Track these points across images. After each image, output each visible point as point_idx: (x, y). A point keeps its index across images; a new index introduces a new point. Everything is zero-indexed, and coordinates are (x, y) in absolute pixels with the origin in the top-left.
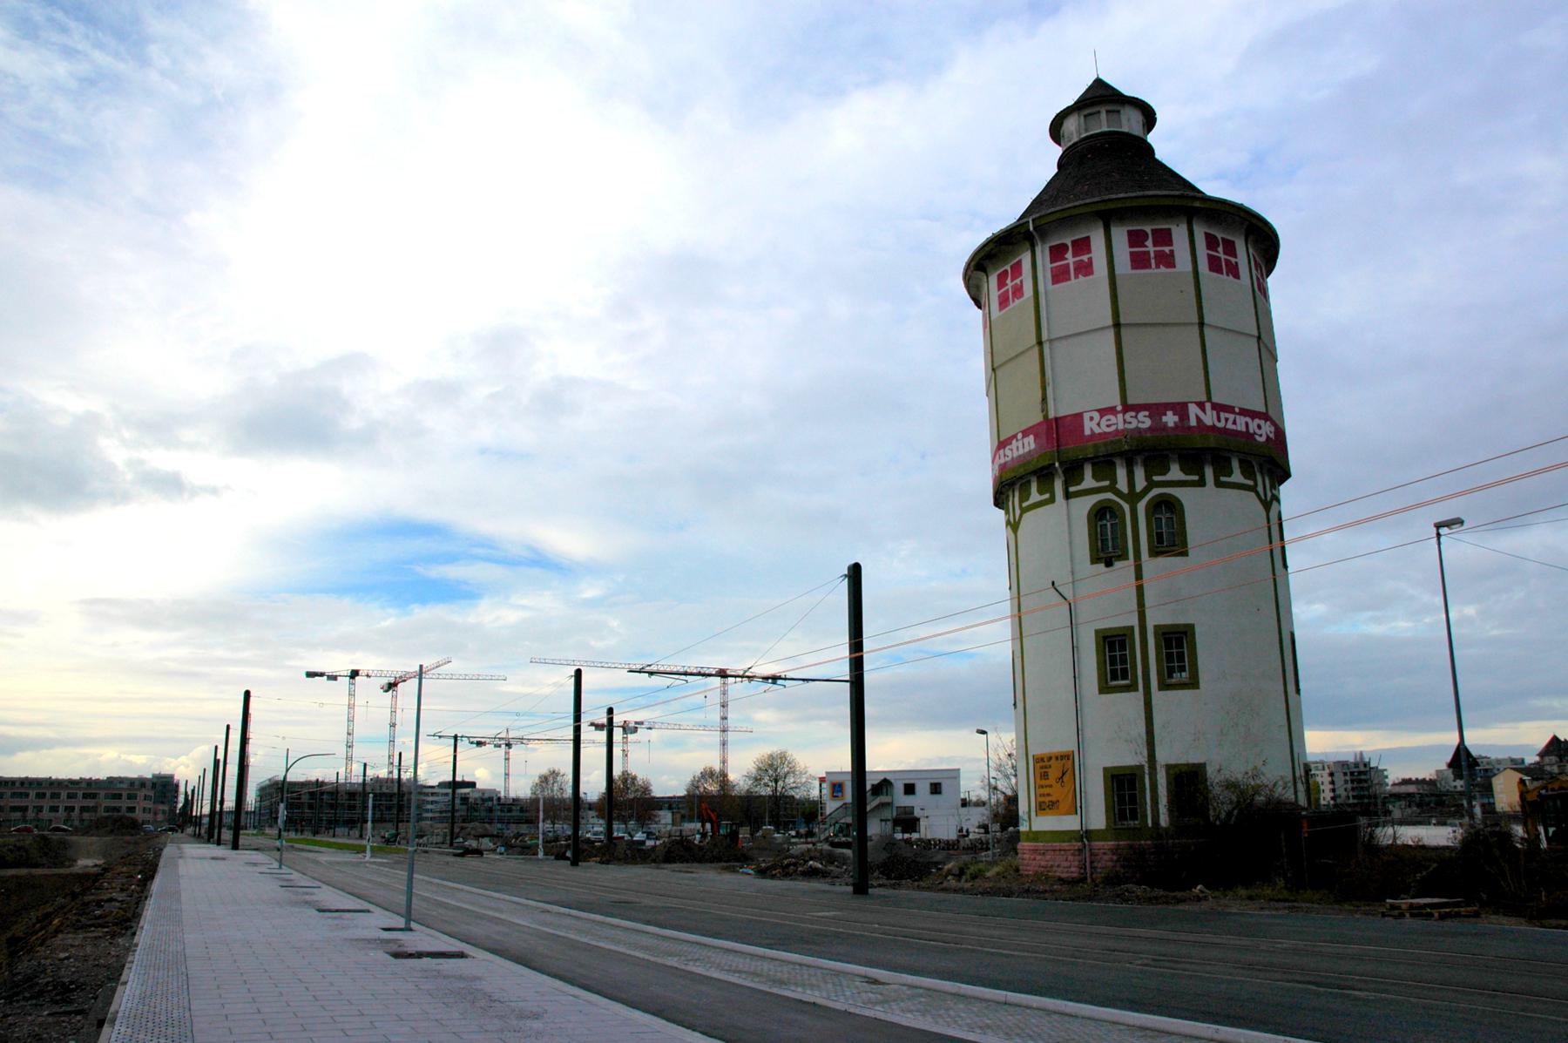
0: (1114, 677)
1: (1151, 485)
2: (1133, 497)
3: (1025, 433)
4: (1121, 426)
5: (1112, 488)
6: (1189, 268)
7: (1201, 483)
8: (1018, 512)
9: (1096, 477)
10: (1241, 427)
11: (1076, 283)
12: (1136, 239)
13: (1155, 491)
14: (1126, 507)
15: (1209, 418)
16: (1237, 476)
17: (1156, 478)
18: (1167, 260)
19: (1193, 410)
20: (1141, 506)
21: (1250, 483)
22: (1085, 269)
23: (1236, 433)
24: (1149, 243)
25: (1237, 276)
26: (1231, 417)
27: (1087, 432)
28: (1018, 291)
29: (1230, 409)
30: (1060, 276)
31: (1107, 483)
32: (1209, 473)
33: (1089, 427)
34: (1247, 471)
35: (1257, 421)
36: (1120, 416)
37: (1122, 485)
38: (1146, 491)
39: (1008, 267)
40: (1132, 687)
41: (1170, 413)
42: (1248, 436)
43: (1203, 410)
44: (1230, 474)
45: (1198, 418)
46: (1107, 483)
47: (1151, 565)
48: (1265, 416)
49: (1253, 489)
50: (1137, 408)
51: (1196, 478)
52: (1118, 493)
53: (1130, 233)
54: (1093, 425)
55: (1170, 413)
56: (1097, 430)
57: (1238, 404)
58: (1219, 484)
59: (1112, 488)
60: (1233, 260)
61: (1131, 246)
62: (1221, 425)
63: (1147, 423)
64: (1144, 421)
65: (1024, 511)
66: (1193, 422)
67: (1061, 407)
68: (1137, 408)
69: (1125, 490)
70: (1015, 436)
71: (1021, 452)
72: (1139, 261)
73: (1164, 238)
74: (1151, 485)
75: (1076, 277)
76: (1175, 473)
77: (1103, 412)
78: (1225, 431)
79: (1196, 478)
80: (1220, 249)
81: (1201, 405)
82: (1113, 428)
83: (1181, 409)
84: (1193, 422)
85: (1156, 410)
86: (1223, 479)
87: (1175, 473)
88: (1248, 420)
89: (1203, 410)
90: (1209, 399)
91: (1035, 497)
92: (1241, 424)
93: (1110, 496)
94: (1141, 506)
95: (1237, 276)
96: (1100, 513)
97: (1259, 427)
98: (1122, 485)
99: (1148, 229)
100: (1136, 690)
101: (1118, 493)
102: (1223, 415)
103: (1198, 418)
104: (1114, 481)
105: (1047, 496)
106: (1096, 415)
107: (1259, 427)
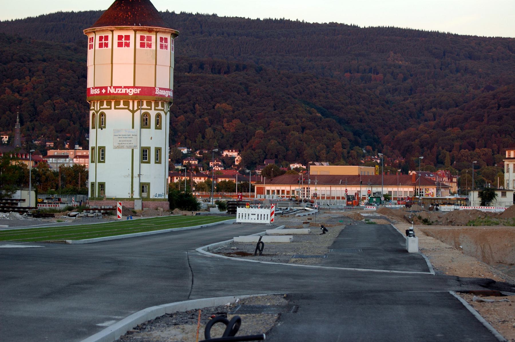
0: (144, 159)
1: (100, 109)
2: (97, 112)
7: (110, 108)
13: (101, 111)
15: (112, 91)
16: (122, 106)
19: (109, 88)
20: (98, 114)
26: (120, 89)
29: (121, 87)
34: (126, 103)
35: (130, 89)
37: (96, 109)
38: (99, 110)
42: (126, 94)
44: (119, 105)
47: (99, 130)
48: (134, 87)
49: (128, 109)
57: (123, 86)
58: (115, 108)
64: (97, 91)
66: (108, 92)
76: (105, 106)
78: (117, 94)
81: (110, 87)
83: (106, 88)
84: (108, 92)
85: (101, 88)
87: (105, 106)
88: (127, 89)
90: (112, 85)
92: (124, 91)
93: (94, 111)
94: (98, 114)
97: (131, 91)
102: (117, 89)
107: (131, 91)
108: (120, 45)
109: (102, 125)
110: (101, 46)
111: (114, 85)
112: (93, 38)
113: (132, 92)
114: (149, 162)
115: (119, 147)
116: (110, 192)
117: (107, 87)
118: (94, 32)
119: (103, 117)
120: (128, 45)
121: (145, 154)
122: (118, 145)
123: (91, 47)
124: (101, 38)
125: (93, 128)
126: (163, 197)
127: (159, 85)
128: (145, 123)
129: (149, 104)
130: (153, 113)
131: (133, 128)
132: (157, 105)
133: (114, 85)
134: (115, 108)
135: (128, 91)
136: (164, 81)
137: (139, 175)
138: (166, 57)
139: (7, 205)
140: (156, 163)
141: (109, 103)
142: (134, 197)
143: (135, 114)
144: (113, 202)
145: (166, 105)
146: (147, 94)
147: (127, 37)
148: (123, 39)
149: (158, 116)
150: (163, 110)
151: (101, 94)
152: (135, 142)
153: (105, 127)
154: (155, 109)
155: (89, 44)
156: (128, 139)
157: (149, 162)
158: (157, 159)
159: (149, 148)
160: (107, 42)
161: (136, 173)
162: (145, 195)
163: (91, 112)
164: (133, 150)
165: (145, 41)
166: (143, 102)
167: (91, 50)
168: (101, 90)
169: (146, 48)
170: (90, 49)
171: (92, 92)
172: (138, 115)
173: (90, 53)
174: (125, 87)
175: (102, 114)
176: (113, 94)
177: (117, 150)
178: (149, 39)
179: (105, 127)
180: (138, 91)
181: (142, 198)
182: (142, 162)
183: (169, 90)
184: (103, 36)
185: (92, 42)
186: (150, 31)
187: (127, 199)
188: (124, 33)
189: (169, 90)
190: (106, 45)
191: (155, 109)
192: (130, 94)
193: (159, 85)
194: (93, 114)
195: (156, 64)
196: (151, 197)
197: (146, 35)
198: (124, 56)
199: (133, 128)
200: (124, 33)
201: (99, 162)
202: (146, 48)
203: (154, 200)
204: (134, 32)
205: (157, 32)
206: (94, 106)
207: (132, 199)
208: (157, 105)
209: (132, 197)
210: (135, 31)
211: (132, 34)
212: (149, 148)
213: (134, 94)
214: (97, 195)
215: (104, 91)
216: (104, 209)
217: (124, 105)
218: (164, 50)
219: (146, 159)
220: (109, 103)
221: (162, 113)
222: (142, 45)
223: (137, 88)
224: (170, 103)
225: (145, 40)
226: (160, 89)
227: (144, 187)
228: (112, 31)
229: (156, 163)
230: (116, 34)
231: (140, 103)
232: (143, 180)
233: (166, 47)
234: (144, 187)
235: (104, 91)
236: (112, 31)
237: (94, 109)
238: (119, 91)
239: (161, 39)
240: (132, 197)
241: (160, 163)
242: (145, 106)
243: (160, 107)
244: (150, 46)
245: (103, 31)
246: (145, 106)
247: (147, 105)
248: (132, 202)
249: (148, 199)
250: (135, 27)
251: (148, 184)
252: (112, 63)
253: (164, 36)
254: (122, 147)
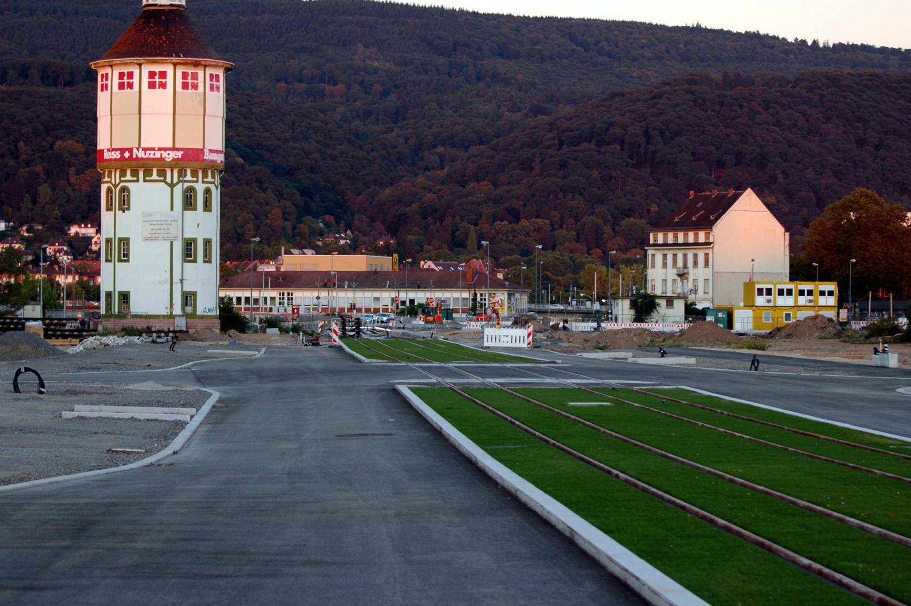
1: (121, 181)
2: (116, 186)
7: (137, 181)
13: (122, 184)
15: (141, 154)
16: (155, 176)
19: (135, 151)
20: (118, 189)
26: (153, 152)
29: (153, 149)
34: (162, 173)
37: (113, 181)
42: (162, 159)
44: (151, 175)
47: (119, 213)
48: (174, 149)
49: (165, 181)
57: (156, 146)
58: (145, 181)
64: (117, 155)
66: (134, 156)
74: (121, 181)
77: (109, 150)
78: (148, 159)
81: (138, 149)
83: (130, 150)
85: (122, 151)
88: (163, 152)
92: (158, 155)
93: (110, 185)
94: (118, 189)
102: (148, 152)
108: (152, 85)
109: (125, 204)
110: (121, 86)
111: (143, 145)
112: (107, 74)
113: (170, 156)
114: (195, 261)
115: (152, 238)
116: (137, 306)
118: (111, 66)
119: (126, 194)
120: (163, 86)
121: (189, 246)
123: (105, 88)
124: (121, 75)
125: (109, 209)
126: (214, 313)
127: (208, 146)
128: (189, 202)
129: (194, 173)
130: (200, 188)
131: (172, 209)
132: (205, 175)
133: (143, 145)
134: (145, 181)
135: (165, 154)
136: (214, 140)
137: (182, 281)
138: (217, 102)
139: (52, 327)
140: (205, 262)
141: (135, 173)
142: (174, 313)
143: (175, 189)
144: (143, 320)
145: (217, 176)
146: (191, 159)
147: (163, 75)
148: (157, 77)
149: (208, 191)
150: (213, 183)
151: (123, 158)
152: (175, 231)
153: (128, 209)
154: (203, 182)
155: (99, 83)
156: (165, 227)
157: (195, 261)
158: (205, 256)
159: (195, 240)
160: (131, 81)
161: (177, 278)
162: (189, 310)
163: (104, 188)
164: (172, 243)
165: (189, 80)
166: (185, 171)
167: (105, 92)
168: (122, 154)
169: (191, 91)
170: (102, 90)
171: (107, 156)
172: (178, 191)
173: (103, 98)
174: (160, 149)
175: (124, 189)
176: (142, 159)
177: (148, 242)
178: (195, 76)
179: (128, 209)
180: (179, 154)
181: (185, 314)
182: (185, 261)
183: (221, 152)
184: (126, 71)
185: (107, 80)
186: (196, 65)
187: (164, 316)
188: (157, 68)
189: (221, 152)
190: (130, 86)
191: (203, 182)
193: (208, 146)
194: (109, 190)
195: (204, 115)
196: (199, 313)
197: (190, 70)
198: (158, 102)
199: (172, 209)
200: (157, 68)
201: (120, 261)
202: (190, 91)
203: (202, 317)
204: (172, 67)
205: (205, 66)
206: (110, 176)
207: (171, 316)
208: (205, 175)
209: (171, 313)
210: (175, 65)
211: (169, 69)
212: (195, 240)
213: (174, 160)
214: (117, 310)
215: (127, 155)
216: (174, 332)
217: (158, 175)
218: (215, 93)
220: (135, 173)
221: (212, 187)
222: (185, 86)
223: (178, 150)
224: (221, 171)
225: (189, 78)
226: (211, 151)
227: (188, 298)
228: (140, 65)
229: (205, 262)
230: (146, 69)
231: (182, 173)
232: (188, 288)
233: (218, 88)
234: (188, 298)
235: (127, 155)
236: (140, 65)
237: (110, 182)
238: (151, 155)
239: (211, 75)
240: (171, 313)
241: (209, 261)
242: (189, 177)
243: (210, 179)
244: (195, 87)
245: (125, 64)
246: (189, 177)
247: (192, 176)
248: (172, 320)
249: (193, 315)
250: (175, 59)
251: (194, 294)
252: (140, 113)
253: (215, 72)
254: (156, 239)
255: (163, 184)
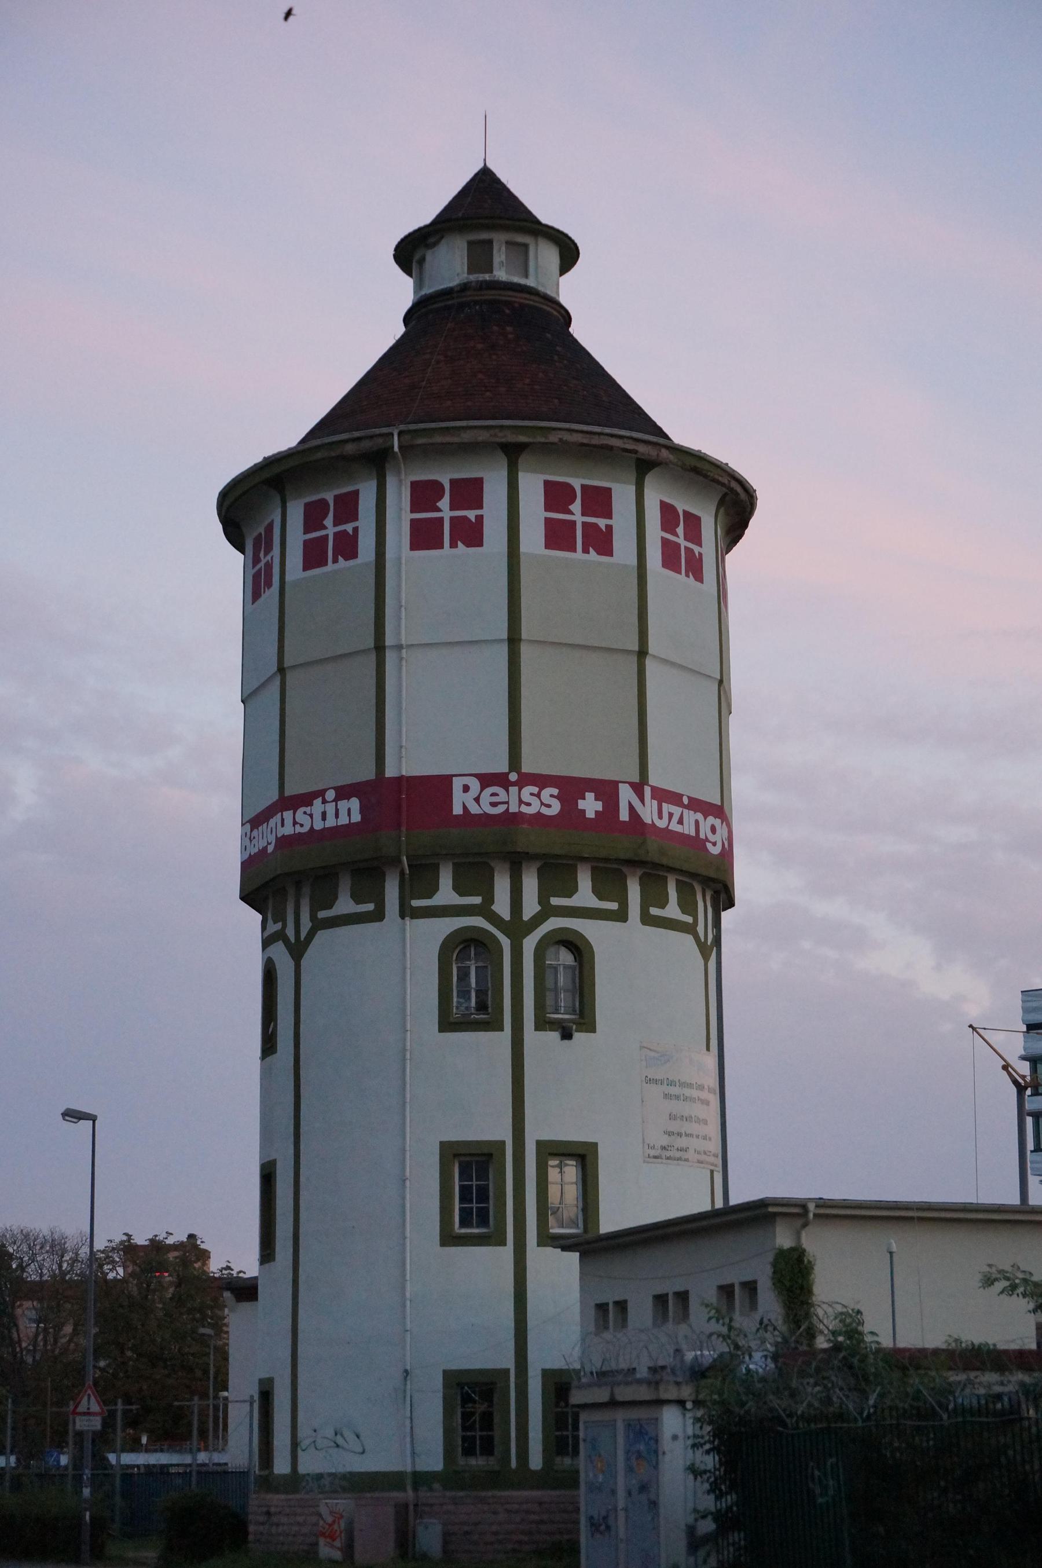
1: (547, 912)
2: (517, 929)
3: (343, 793)
4: (514, 808)
5: (485, 910)
6: (633, 561)
7: (621, 916)
8: (306, 925)
9: (459, 889)
10: (688, 829)
11: (450, 556)
12: (557, 496)
14: (505, 942)
15: (648, 812)
16: (672, 910)
17: (555, 901)
18: (601, 542)
19: (626, 794)
20: (529, 944)
21: (689, 919)
22: (471, 534)
23: (683, 838)
24: (576, 507)
25: (699, 578)
26: (677, 811)
27: (457, 810)
28: (347, 546)
29: (675, 798)
30: (424, 536)
31: (477, 900)
32: (634, 892)
33: (459, 802)
35: (711, 820)
36: (514, 790)
37: (502, 907)
38: (538, 920)
39: (329, 496)
40: (497, 1239)
41: (590, 796)
43: (642, 800)
45: (631, 808)
46: (477, 900)
50: (541, 781)
51: (614, 906)
52: (494, 919)
53: (550, 487)
54: (469, 799)
55: (590, 796)
56: (474, 809)
57: (688, 790)
58: (647, 919)
59: (485, 910)
60: (696, 549)
61: (547, 508)
62: (661, 824)
63: (556, 808)
65: (319, 925)
66: (624, 815)
67: (410, 759)
68: (541, 781)
69: (506, 915)
70: (321, 793)
71: (331, 822)
72: (558, 536)
73: (599, 502)
75: (453, 545)
76: (585, 896)
77: (487, 780)
79: (614, 906)
80: (680, 530)
81: (638, 788)
82: (500, 809)
83: (607, 791)
84: (624, 815)
85: (571, 788)
86: (654, 911)
87: (585, 896)
88: (699, 816)
89: (642, 800)
91: (345, 905)
94: (529, 944)
95: (699, 578)
96: (464, 946)
97: (713, 830)
98: (502, 907)
99: (577, 483)
100: (503, 1243)
101: (494, 919)
103: (631, 808)
104: (489, 898)
105: (370, 907)
106: (475, 784)
107: (713, 830)
117: (616, 784)
122: (665, 1140)
131: (708, 1049)
133: (654, 780)
175: (579, 948)
192: (709, 846)
219: (464, 1223)
235: (590, 805)
255: (689, 939)
